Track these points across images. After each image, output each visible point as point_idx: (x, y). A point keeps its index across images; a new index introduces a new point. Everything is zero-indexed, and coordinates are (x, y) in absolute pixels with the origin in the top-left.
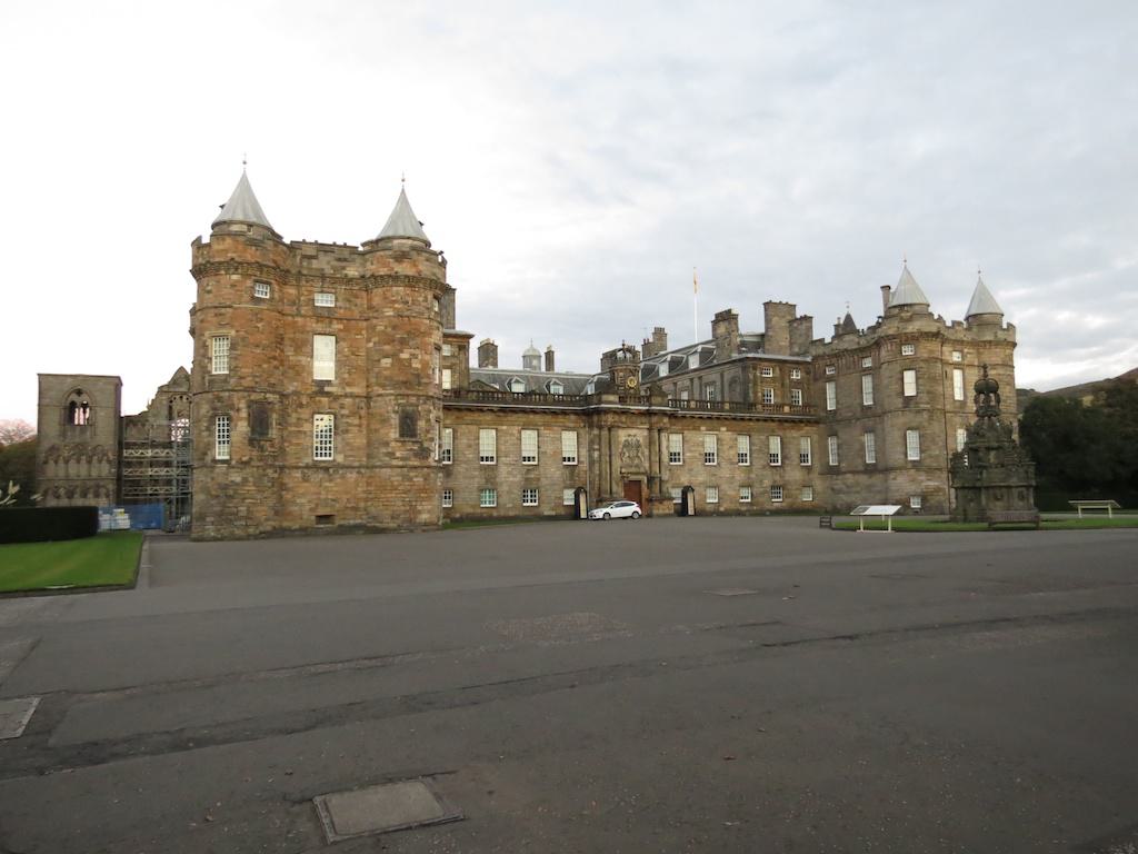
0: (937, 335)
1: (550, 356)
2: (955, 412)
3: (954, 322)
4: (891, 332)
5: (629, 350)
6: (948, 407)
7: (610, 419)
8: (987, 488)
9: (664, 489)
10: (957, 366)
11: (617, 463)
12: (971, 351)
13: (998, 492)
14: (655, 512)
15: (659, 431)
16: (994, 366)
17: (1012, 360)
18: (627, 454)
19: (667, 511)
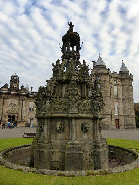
0: (107, 74)
1: (32, 88)
2: (114, 98)
3: (114, 72)
4: (94, 73)
5: (16, 76)
6: (112, 96)
7: (4, 96)
8: (51, 118)
9: (22, 118)
10: (115, 85)
11: (6, 110)
12: (119, 81)
13: (59, 124)
14: (18, 126)
15: (23, 100)
16: (126, 85)
17: (132, 84)
18: (10, 107)
19: (22, 126)
